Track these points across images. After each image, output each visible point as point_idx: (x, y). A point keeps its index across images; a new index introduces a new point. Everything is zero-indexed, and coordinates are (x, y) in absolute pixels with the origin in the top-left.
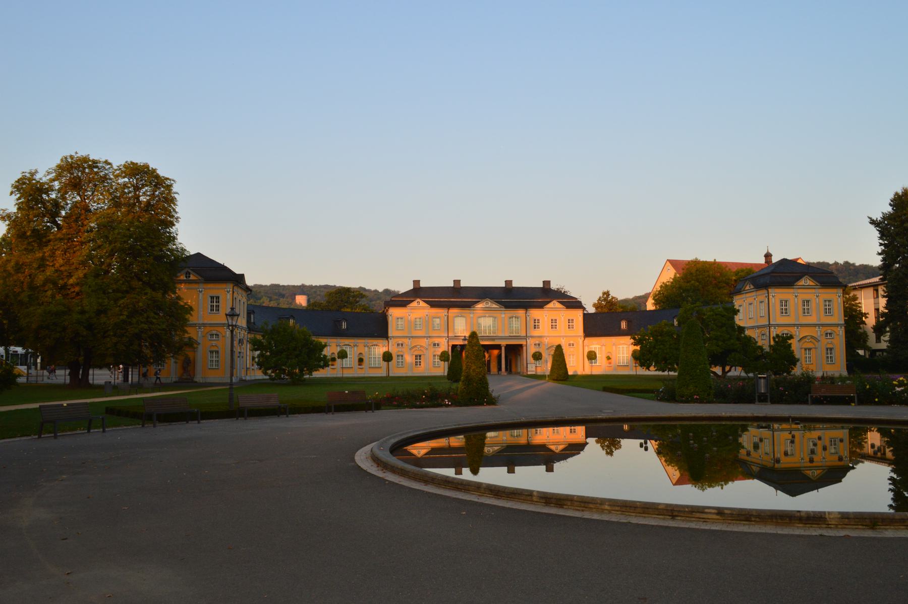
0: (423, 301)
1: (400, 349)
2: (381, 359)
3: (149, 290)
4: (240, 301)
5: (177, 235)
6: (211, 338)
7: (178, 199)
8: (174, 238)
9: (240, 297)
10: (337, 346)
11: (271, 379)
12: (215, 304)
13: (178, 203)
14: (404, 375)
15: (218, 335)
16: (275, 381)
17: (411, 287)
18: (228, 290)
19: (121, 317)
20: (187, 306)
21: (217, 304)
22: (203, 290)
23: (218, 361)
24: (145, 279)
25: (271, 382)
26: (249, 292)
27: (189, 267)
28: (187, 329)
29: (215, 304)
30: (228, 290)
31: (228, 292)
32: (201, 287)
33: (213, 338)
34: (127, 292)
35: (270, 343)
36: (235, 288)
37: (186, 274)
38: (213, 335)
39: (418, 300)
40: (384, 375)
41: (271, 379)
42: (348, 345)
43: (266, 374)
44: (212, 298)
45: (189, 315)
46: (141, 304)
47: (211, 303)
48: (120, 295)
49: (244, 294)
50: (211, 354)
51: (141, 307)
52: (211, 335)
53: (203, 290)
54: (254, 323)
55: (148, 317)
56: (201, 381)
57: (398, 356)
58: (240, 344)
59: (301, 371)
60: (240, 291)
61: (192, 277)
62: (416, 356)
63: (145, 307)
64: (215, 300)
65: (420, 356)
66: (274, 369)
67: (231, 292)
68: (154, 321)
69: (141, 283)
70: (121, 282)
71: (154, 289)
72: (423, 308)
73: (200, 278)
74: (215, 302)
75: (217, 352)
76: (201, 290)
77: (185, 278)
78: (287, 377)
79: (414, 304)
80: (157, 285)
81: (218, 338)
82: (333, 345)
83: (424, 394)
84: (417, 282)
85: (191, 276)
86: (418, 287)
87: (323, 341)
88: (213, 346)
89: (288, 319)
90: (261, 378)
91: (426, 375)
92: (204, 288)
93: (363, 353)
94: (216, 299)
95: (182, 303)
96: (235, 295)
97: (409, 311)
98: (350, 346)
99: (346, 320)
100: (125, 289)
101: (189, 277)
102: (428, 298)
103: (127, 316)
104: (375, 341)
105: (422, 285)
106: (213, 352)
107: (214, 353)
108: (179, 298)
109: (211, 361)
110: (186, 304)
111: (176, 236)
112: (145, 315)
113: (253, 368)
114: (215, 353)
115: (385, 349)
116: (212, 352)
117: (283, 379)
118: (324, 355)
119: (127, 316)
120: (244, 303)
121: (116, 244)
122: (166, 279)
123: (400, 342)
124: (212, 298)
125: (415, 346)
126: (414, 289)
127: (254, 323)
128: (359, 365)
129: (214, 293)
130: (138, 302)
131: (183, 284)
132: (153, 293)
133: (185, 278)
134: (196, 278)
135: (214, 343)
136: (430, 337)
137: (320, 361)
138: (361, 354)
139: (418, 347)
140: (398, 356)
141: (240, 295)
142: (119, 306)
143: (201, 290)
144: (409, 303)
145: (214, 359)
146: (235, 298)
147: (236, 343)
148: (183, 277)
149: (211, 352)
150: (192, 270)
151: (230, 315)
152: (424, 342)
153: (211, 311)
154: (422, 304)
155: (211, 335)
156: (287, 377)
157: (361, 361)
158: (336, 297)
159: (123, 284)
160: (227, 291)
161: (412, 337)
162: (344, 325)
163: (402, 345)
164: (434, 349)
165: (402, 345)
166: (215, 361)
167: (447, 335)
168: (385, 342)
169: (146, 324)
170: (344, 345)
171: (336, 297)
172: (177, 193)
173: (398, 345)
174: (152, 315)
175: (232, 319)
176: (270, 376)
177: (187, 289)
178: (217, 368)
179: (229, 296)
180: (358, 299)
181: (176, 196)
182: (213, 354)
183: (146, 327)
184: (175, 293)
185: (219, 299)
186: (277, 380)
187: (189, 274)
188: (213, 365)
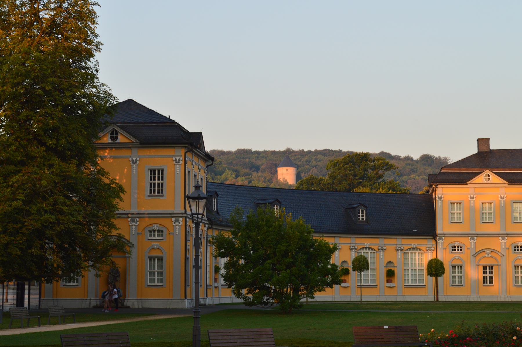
0: (495, 173)
1: (456, 255)
2: (425, 272)
3: (56, 161)
4: (195, 176)
5: (97, 71)
6: (151, 236)
7: (98, 14)
8: (93, 77)
9: (195, 170)
10: (350, 249)
11: (248, 303)
12: (157, 181)
13: (98, 20)
14: (464, 299)
15: (162, 232)
16: (254, 307)
17: (474, 151)
18: (178, 158)
19: (15, 203)
20: (113, 186)
21: (160, 181)
22: (138, 159)
23: (162, 273)
24: (50, 142)
25: (247, 307)
26: (210, 162)
27: (115, 123)
28: (116, 222)
29: (157, 181)
30: (178, 158)
31: (178, 162)
32: (135, 155)
33: (154, 235)
34: (23, 163)
35: (245, 245)
36: (189, 155)
37: (112, 134)
38: (154, 231)
39: (487, 172)
40: (431, 298)
41: (248, 303)
42: (369, 248)
43: (238, 295)
44: (152, 171)
45: (118, 200)
46: (44, 182)
47: (151, 179)
48: (12, 168)
49: (202, 165)
50: (150, 262)
51: (45, 187)
52: (151, 231)
53: (138, 159)
54: (217, 212)
55: (55, 203)
56: (136, 307)
57: (453, 267)
59: (296, 290)
60: (196, 160)
61: (121, 139)
62: (484, 268)
63: (50, 187)
64: (157, 175)
65: (491, 267)
66: (252, 286)
67: (182, 162)
68: (65, 208)
69: (43, 148)
70: (13, 148)
71: (64, 158)
72: (495, 186)
73: (133, 140)
74: (157, 178)
75: (161, 259)
76: (134, 159)
77: (110, 141)
78: (273, 301)
79: (481, 179)
80: (69, 153)
81: (162, 236)
83: (515, 333)
84: (483, 142)
85: (120, 137)
86: (485, 150)
87: (330, 241)
88: (153, 248)
89: (272, 204)
90: (228, 301)
91: (502, 299)
92: (138, 156)
94: (159, 174)
95: (107, 181)
96: (189, 167)
98: (372, 249)
99: (365, 207)
100: (19, 158)
101: (116, 138)
102: (504, 168)
103: (23, 201)
104: (413, 242)
105: (493, 146)
106: (154, 260)
107: (156, 260)
108: (102, 172)
109: (150, 273)
110: (113, 181)
111: (95, 73)
112: (51, 199)
113: (216, 285)
114: (158, 260)
115: (430, 256)
116: (152, 259)
117: (266, 303)
118: (334, 265)
119: (23, 201)
120: (202, 179)
121: (5, 88)
122: (82, 142)
123: (457, 244)
124: (152, 171)
125: (483, 251)
126: (478, 152)
127: (217, 212)
128: (388, 281)
129: (156, 164)
130: (40, 180)
131: (107, 151)
132: (62, 164)
133: (110, 141)
134: (127, 141)
135: (156, 244)
136: (508, 235)
137: (327, 275)
138: (390, 262)
139: (488, 251)
140: (453, 267)
141: (196, 167)
142: (12, 186)
143: (134, 159)
144: (472, 178)
145: (156, 270)
146: (189, 172)
148: (107, 139)
149: (150, 259)
150: (120, 127)
151: (194, 198)
152: (500, 245)
153: (151, 193)
154: (495, 179)
155: (151, 231)
156: (273, 301)
157: (390, 274)
158: (345, 169)
159: (16, 150)
160: (176, 160)
161: (477, 235)
162: (362, 215)
163: (460, 248)
164: (515, 254)
165: (460, 248)
166: (158, 273)
168: (429, 243)
169: (52, 214)
170: (363, 248)
171: (345, 169)
172: (96, 4)
173: (453, 248)
174: (62, 199)
175: (198, 206)
176: (245, 298)
177: (114, 158)
178: (160, 284)
179: (179, 169)
180: (380, 172)
181: (95, 8)
182: (154, 262)
183: (52, 218)
184: (95, 164)
185: (162, 173)
186: (256, 305)
187: (117, 133)
188: (154, 280)
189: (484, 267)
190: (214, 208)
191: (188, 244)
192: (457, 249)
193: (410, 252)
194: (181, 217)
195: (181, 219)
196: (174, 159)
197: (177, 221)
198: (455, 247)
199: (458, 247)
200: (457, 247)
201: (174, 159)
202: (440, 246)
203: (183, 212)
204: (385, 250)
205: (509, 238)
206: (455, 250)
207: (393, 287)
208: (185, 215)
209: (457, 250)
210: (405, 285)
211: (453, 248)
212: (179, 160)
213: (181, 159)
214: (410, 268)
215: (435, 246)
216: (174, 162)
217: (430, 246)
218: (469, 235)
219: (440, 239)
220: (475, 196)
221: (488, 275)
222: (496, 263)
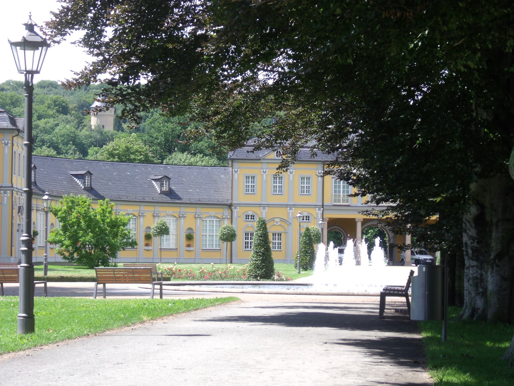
1: (249, 223)
4: (19, 154)
9: (20, 150)
18: (6, 142)
30: (6, 142)
31: (6, 144)
58: (20, 214)
67: (10, 145)
82: (149, 215)
93: (194, 228)
97: (265, 165)
123: (250, 213)
139: (276, 220)
146: (15, 152)
147: (15, 211)
160: (5, 143)
161: (269, 205)
163: (253, 217)
165: (253, 217)
167: (321, 204)
173: (247, 217)
179: (7, 150)
189: (273, 234)
190: (33, 180)
191: (14, 212)
192: (250, 217)
193: (208, 219)
194: (9, 190)
195: (9, 192)
196: (3, 142)
197: (5, 193)
198: (249, 216)
199: (251, 216)
200: (250, 216)
201: (3, 142)
202: (235, 215)
203: (11, 186)
204: (185, 217)
205: (297, 209)
206: (248, 219)
207: (192, 251)
208: (12, 189)
209: (250, 218)
210: (202, 249)
211: (247, 217)
212: (8, 143)
213: (10, 142)
214: (208, 234)
215: (230, 215)
216: (4, 145)
217: (227, 214)
218: (261, 206)
219: (235, 209)
220: (267, 170)
221: (277, 241)
222: (283, 230)
